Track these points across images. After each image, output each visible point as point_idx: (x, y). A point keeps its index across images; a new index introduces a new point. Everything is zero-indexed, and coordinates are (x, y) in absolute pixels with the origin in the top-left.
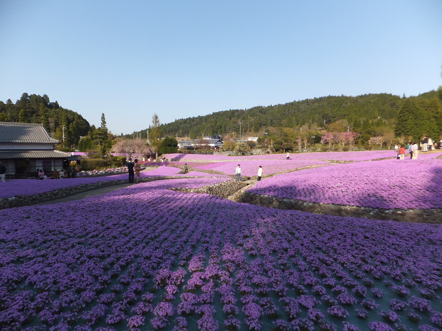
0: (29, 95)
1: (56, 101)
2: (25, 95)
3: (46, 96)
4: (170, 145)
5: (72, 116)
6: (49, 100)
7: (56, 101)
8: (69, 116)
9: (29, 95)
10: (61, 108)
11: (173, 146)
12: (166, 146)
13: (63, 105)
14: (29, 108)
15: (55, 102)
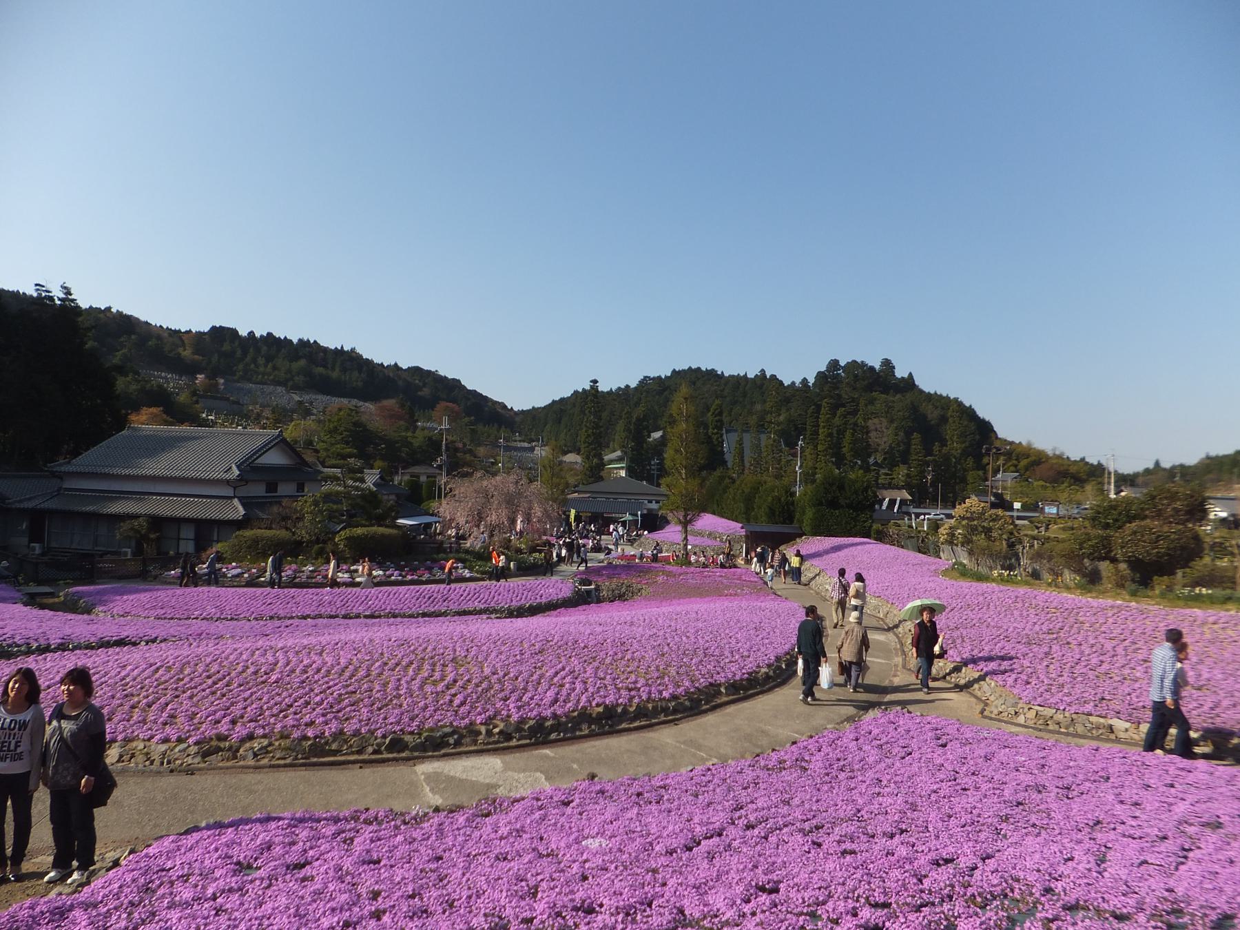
0: (842, 363)
1: (910, 374)
2: (834, 364)
3: (887, 364)
4: (833, 504)
5: (937, 413)
6: (893, 372)
7: (910, 374)
8: (929, 412)
9: (842, 363)
10: (921, 392)
11: (849, 506)
12: (821, 504)
13: (926, 384)
14: (832, 397)
15: (906, 376)
